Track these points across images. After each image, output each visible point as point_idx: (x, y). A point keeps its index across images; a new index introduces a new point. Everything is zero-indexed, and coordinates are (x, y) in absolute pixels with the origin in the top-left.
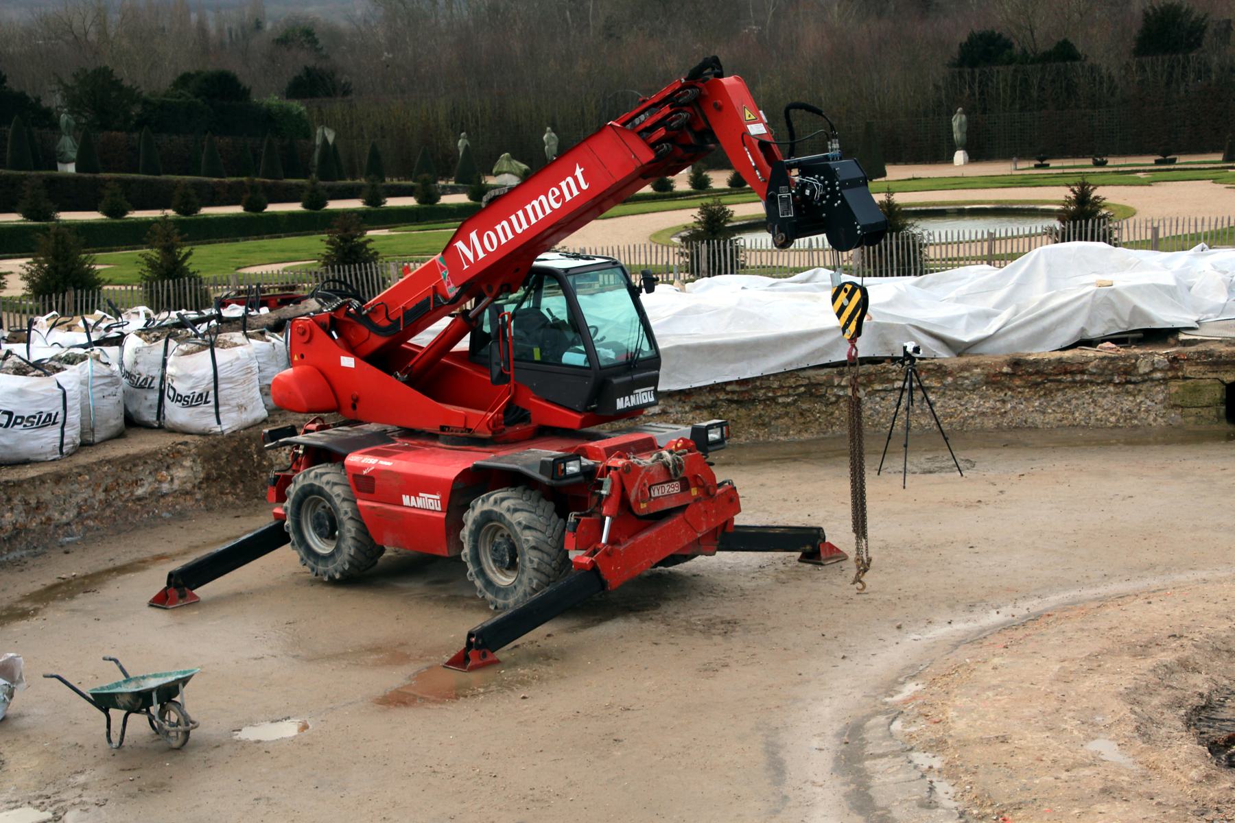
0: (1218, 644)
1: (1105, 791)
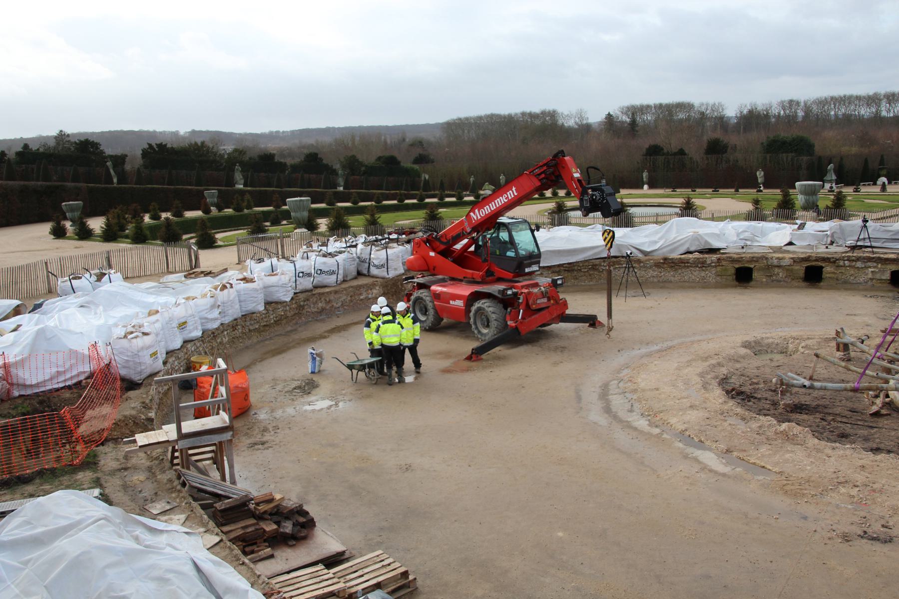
1: (691, 407)
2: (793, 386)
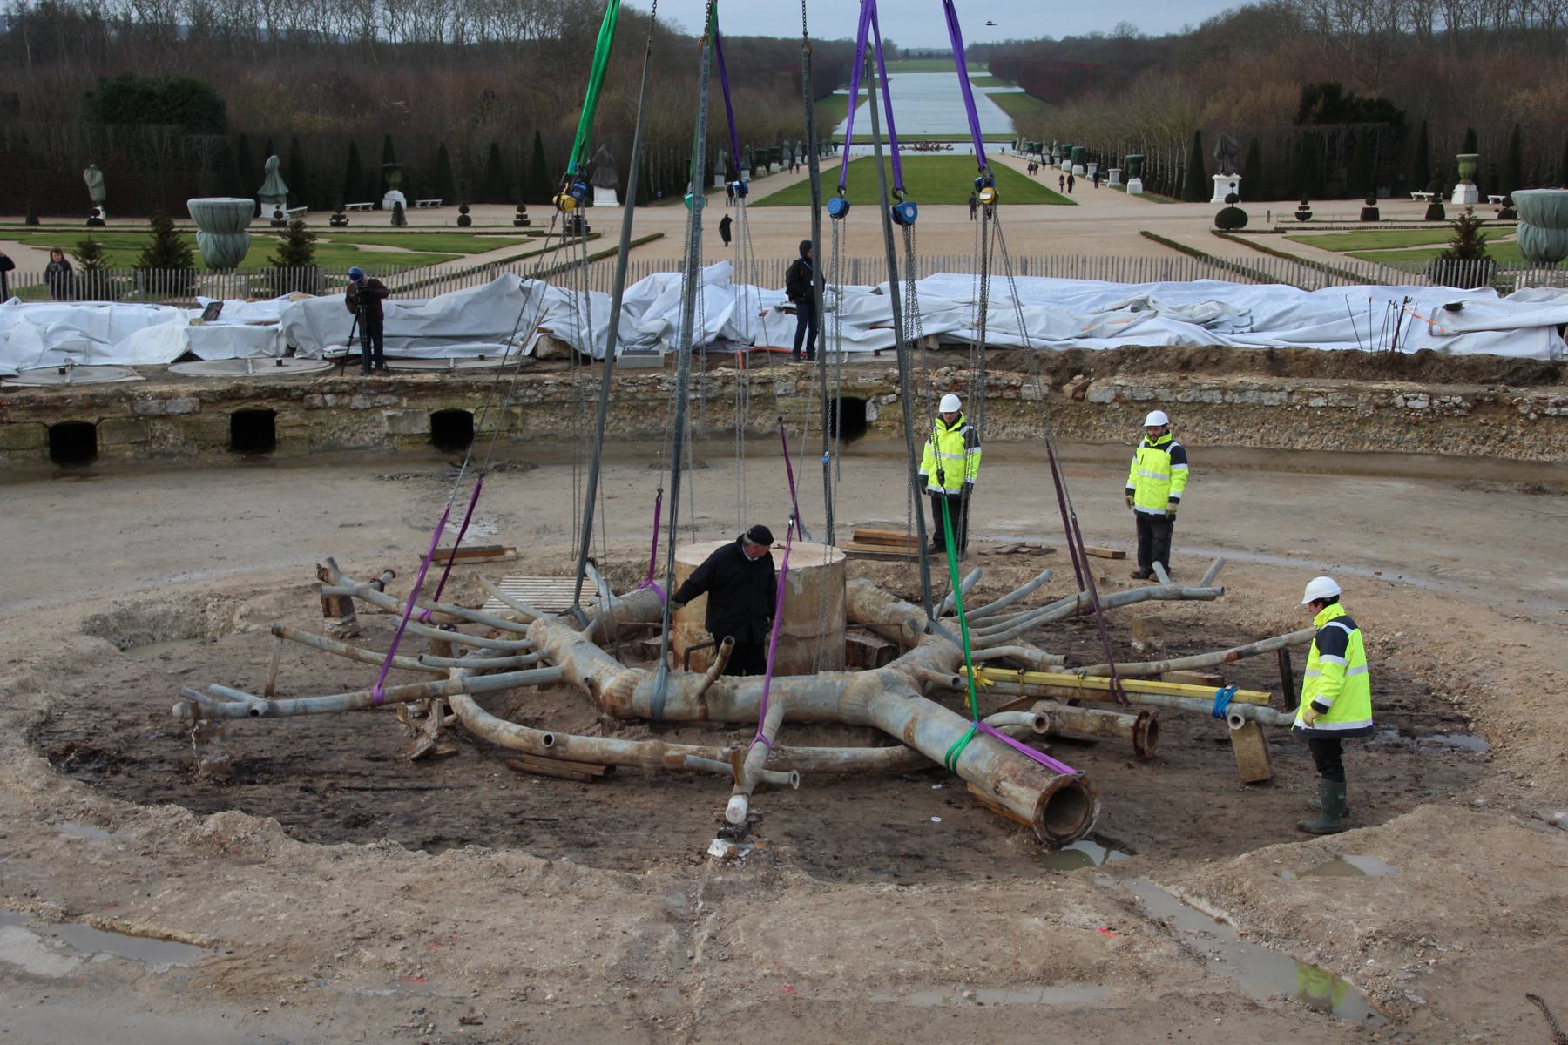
0: (56, 664)
2: (226, 716)
